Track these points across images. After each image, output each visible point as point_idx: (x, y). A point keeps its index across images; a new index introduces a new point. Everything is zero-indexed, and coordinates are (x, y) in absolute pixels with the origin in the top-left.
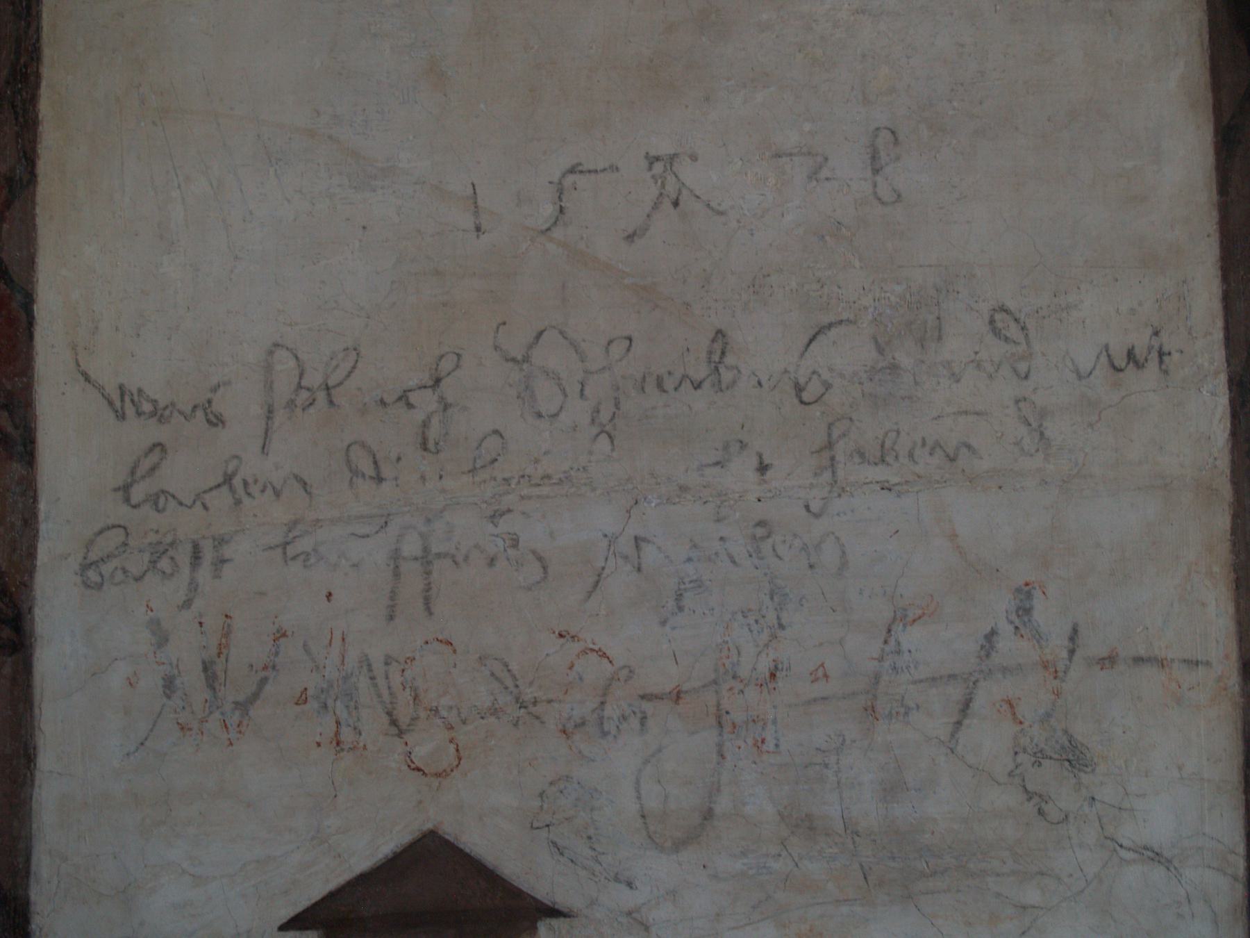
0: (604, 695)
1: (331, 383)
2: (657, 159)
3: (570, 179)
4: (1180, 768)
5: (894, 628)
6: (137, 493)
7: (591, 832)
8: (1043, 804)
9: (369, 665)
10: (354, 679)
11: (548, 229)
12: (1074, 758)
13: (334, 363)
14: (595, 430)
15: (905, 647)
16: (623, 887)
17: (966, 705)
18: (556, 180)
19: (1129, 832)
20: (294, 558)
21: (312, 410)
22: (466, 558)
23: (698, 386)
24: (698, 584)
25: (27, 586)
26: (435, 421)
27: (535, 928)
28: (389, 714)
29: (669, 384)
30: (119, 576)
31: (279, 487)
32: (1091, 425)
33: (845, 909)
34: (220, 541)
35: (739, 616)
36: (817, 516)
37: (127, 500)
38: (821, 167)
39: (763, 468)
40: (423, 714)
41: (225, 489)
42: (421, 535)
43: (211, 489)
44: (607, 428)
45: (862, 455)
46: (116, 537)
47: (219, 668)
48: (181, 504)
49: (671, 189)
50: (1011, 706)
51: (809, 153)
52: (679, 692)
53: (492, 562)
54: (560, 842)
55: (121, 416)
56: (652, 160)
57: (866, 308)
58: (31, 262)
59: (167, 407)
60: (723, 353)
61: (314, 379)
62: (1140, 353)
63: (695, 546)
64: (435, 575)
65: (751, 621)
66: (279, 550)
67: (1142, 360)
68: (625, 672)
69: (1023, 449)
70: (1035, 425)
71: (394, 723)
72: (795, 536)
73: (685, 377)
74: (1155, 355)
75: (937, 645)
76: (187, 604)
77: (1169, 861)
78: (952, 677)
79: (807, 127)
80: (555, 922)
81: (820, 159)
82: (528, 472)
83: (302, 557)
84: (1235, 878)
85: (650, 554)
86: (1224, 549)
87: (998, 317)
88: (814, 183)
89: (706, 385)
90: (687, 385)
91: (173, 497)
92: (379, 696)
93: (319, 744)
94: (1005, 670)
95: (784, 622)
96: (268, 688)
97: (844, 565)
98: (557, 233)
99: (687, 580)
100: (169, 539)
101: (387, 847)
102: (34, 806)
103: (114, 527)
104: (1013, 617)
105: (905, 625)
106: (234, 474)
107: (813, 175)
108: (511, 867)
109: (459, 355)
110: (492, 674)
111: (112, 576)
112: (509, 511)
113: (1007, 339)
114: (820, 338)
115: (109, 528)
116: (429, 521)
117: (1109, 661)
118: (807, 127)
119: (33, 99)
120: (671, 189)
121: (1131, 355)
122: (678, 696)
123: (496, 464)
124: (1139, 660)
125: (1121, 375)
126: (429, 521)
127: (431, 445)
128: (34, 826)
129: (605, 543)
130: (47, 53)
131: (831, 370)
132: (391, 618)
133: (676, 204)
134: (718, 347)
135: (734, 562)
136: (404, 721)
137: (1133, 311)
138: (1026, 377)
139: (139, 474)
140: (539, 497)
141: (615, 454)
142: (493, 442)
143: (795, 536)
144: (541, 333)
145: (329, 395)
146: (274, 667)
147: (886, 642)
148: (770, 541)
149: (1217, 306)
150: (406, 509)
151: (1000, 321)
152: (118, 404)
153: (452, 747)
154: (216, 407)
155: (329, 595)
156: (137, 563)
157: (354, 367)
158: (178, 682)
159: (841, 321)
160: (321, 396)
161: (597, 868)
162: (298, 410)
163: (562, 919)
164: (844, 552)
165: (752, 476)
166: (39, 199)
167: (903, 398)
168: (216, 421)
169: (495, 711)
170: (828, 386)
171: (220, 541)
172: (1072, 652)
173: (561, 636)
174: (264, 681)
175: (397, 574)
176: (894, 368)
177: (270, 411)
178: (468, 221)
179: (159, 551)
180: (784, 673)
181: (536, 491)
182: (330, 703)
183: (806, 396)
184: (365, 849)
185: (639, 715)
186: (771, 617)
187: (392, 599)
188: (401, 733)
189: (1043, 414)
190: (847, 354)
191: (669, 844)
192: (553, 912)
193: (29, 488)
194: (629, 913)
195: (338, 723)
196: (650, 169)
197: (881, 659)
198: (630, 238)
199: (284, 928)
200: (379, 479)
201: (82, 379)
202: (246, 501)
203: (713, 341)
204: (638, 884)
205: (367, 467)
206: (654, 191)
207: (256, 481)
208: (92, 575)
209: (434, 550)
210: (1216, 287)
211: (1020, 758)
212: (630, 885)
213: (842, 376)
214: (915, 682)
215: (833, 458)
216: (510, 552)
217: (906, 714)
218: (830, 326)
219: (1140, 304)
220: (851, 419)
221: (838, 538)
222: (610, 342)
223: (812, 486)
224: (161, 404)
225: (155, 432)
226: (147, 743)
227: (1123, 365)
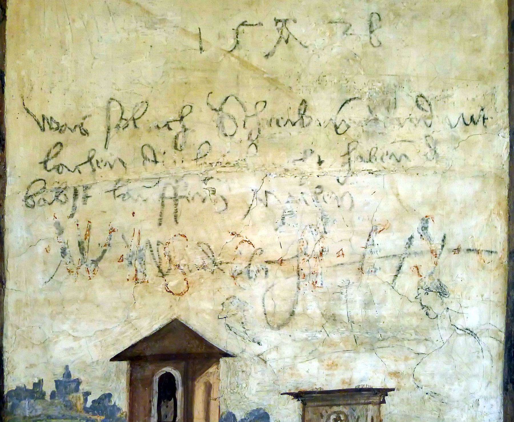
0: (250, 261)
1: (135, 118)
2: (280, 21)
3: (242, 28)
4: (482, 296)
5: (372, 234)
6: (50, 165)
7: (243, 320)
8: (428, 311)
9: (150, 245)
10: (143, 251)
11: (232, 51)
12: (442, 291)
13: (137, 108)
14: (250, 143)
15: (376, 243)
16: (256, 344)
18: (235, 28)
19: (460, 323)
20: (118, 196)
21: (127, 129)
22: (193, 199)
23: (294, 125)
24: (291, 213)
26: (180, 136)
27: (219, 361)
28: (159, 267)
29: (282, 123)
30: (42, 202)
31: (112, 164)
32: (455, 148)
33: (347, 354)
34: (86, 188)
35: (308, 228)
36: (342, 184)
37: (46, 168)
38: (348, 29)
39: (320, 162)
40: (173, 267)
41: (88, 164)
42: (174, 188)
43: (82, 164)
44: (255, 142)
45: (361, 158)
46: (41, 184)
47: (85, 244)
48: (69, 170)
49: (285, 35)
50: (418, 269)
51: (344, 22)
52: (282, 260)
53: (204, 201)
54: (230, 325)
55: (43, 130)
56: (277, 21)
57: (366, 93)
59: (63, 126)
60: (305, 111)
61: (128, 115)
62: (475, 118)
63: (291, 196)
64: (179, 206)
65: (313, 230)
66: (112, 192)
67: (476, 121)
68: (259, 251)
69: (427, 158)
70: (433, 147)
71: (160, 271)
72: (333, 193)
73: (289, 120)
74: (481, 119)
75: (389, 242)
76: (72, 216)
77: (476, 335)
78: (394, 256)
79: (343, 10)
80: (227, 359)
81: (348, 25)
82: (220, 161)
83: (122, 196)
84: (501, 342)
85: (271, 199)
86: (505, 203)
87: (420, 99)
88: (346, 35)
89: (297, 124)
90: (289, 123)
91: (66, 167)
92: (154, 259)
93: (128, 280)
94: (416, 253)
95: (327, 231)
96: (107, 254)
97: (352, 206)
98: (235, 52)
99: (286, 211)
100: (63, 186)
101: (156, 326)
102: (5, 304)
103: (40, 180)
104: (421, 231)
105: (376, 233)
106: (93, 157)
107: (345, 33)
108: (209, 335)
109: (191, 106)
110: (203, 251)
111: (39, 202)
112: (212, 178)
113: (423, 109)
114: (346, 105)
115: (37, 180)
116: (177, 181)
117: (457, 250)
118: (343, 10)
120: (285, 35)
121: (472, 118)
122: (281, 262)
123: (206, 157)
124: (469, 250)
125: (467, 127)
126: (177, 181)
127: (178, 147)
128: (5, 313)
129: (252, 194)
131: (350, 120)
132: (160, 224)
133: (287, 42)
134: (303, 107)
135: (307, 203)
136: (165, 270)
137: (474, 100)
138: (430, 126)
139: (50, 156)
140: (225, 172)
141: (257, 154)
142: (205, 147)
143: (333, 193)
144: (227, 98)
145: (134, 123)
146: (109, 245)
147: (368, 240)
148: (322, 195)
149: (506, 99)
150: (168, 176)
151: (420, 101)
152: (42, 124)
153: (185, 282)
154: (85, 127)
155: (134, 213)
156: (50, 197)
157: (146, 110)
158: (67, 250)
159: (355, 98)
160: (131, 123)
161: (246, 336)
162: (121, 129)
163: (230, 358)
164: (352, 201)
165: (315, 165)
166: (7, 27)
167: (380, 133)
168: (85, 133)
169: (204, 267)
170: (349, 127)
171: (86, 188)
172: (443, 246)
173: (233, 234)
174: (104, 251)
175: (163, 205)
176: (376, 120)
177: (109, 129)
178: (196, 45)
179: (60, 191)
180: (326, 253)
181: (223, 169)
182: (133, 262)
183: (339, 131)
184: (147, 327)
185: (265, 270)
186: (321, 229)
187: (161, 216)
188: (163, 276)
189: (436, 142)
190: (356, 113)
191: (275, 326)
192: (226, 355)
194: (258, 356)
195: (136, 270)
196: (276, 25)
197: (366, 248)
198: (267, 56)
199: (112, 360)
200: (156, 162)
201: (26, 112)
202: (97, 169)
203: (301, 104)
204: (262, 343)
206: (278, 35)
207: (102, 161)
208: (30, 202)
209: (180, 194)
210: (506, 91)
211: (421, 291)
212: (259, 343)
213: (355, 122)
214: (379, 258)
215: (349, 159)
216: (212, 196)
217: (375, 271)
218: (350, 100)
219: (477, 97)
220: (358, 142)
221: (350, 194)
222: (257, 104)
223: (340, 171)
224: (61, 125)
225: (58, 137)
226: (54, 277)
227: (469, 123)
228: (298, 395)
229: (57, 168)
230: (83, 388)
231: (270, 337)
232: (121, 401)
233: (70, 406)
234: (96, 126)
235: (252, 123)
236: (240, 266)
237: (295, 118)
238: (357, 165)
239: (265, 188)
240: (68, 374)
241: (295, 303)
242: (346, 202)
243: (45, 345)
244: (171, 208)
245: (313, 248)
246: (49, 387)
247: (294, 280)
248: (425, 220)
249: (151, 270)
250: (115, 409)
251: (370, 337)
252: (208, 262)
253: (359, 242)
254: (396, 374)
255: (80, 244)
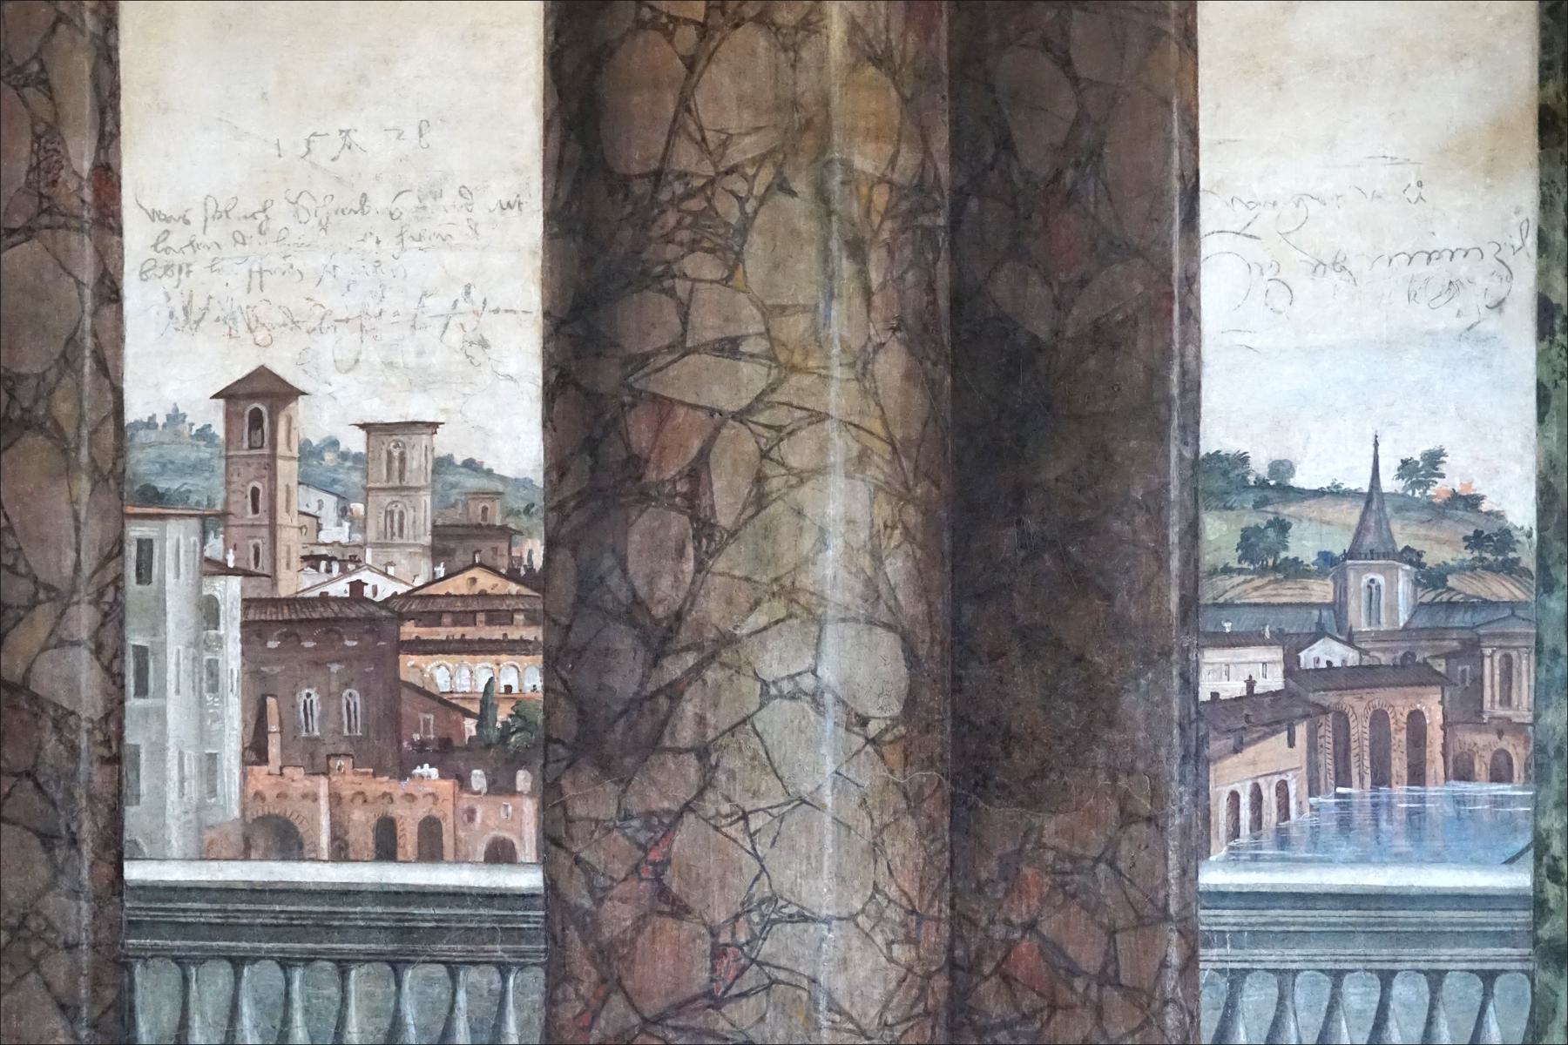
6: (160, 247)
12: (484, 344)
17: (446, 326)
19: (501, 370)
25: (121, 280)
34: (189, 265)
39: (378, 242)
58: (120, 166)
61: (221, 208)
108: (289, 379)
117: (497, 311)
119: (118, 104)
122: (347, 320)
130: (123, 86)
156: (160, 272)
168: (187, 222)
169: (285, 325)
171: (189, 265)
179: (168, 268)
184: (239, 373)
192: (304, 393)
193: (121, 245)
199: (216, 396)
205: (240, 239)
225: (166, 226)
228: (363, 426)
229: (166, 250)
230: (188, 420)
231: (339, 379)
232: (219, 430)
233: (178, 434)
234: (196, 217)
235: (322, 213)
236: (313, 323)
237: (357, 207)
238: (408, 243)
239: (333, 262)
240: (177, 410)
241: (360, 353)
242: (401, 273)
243: (157, 386)
244: (257, 279)
245: (374, 309)
246: (161, 420)
247: (357, 335)
248: (468, 287)
249: (242, 327)
250: (214, 436)
251: (423, 381)
252: (288, 321)
253: (412, 305)
254: (445, 411)
255: (185, 309)
